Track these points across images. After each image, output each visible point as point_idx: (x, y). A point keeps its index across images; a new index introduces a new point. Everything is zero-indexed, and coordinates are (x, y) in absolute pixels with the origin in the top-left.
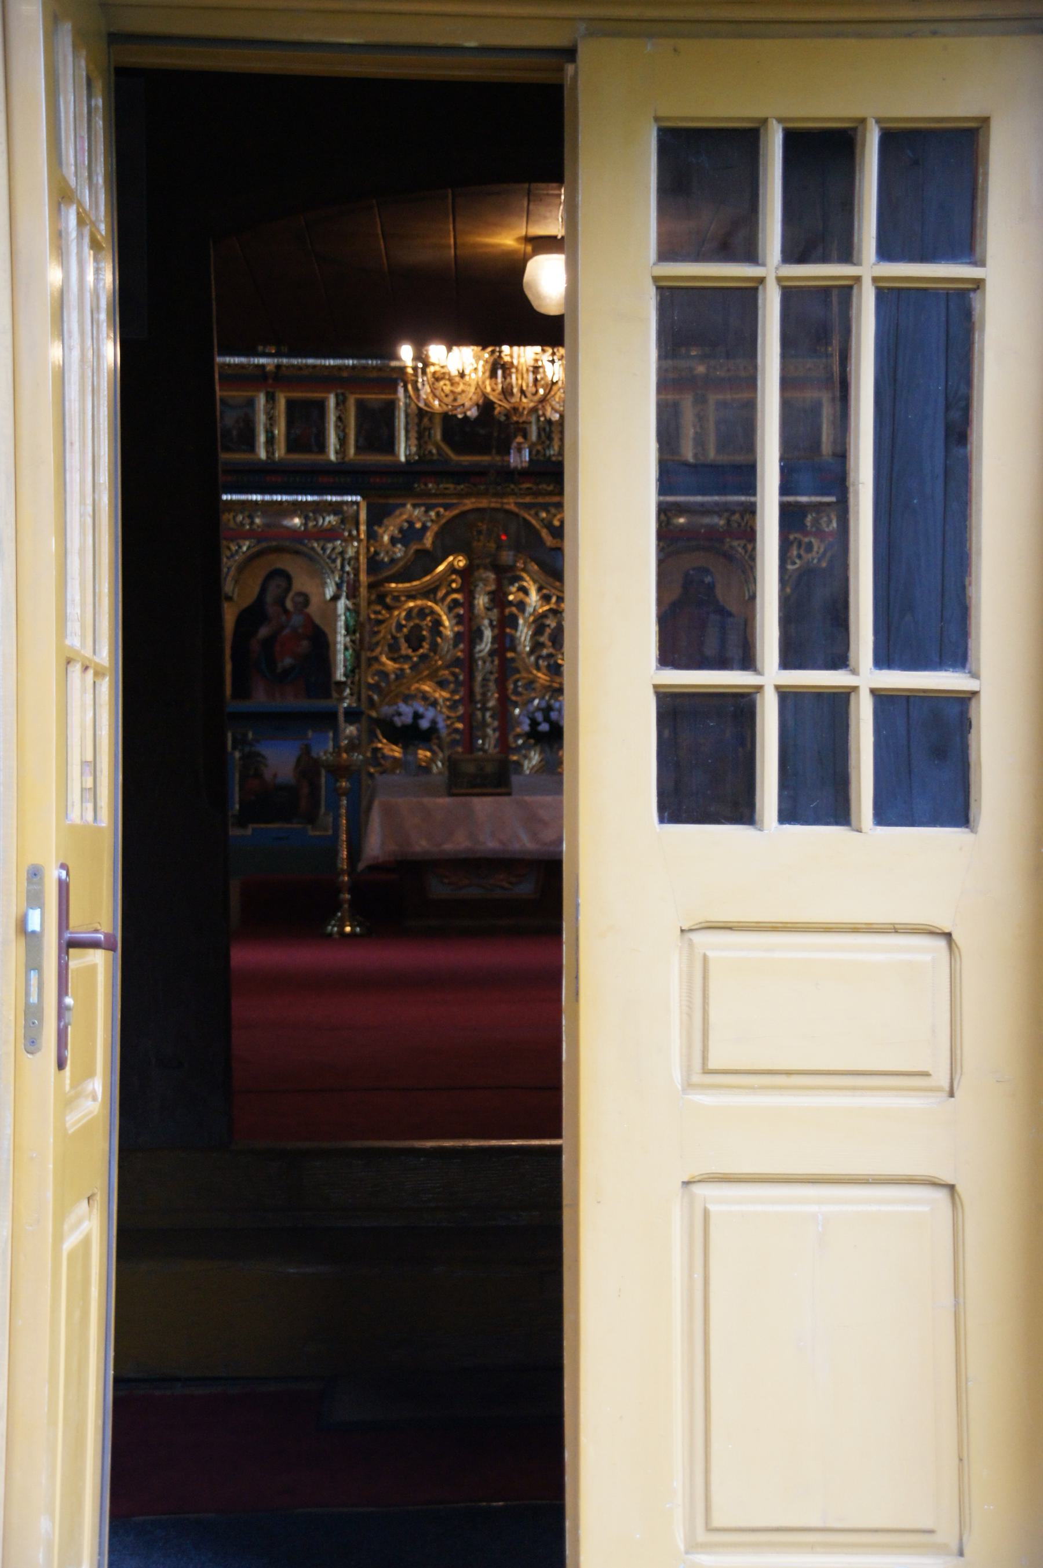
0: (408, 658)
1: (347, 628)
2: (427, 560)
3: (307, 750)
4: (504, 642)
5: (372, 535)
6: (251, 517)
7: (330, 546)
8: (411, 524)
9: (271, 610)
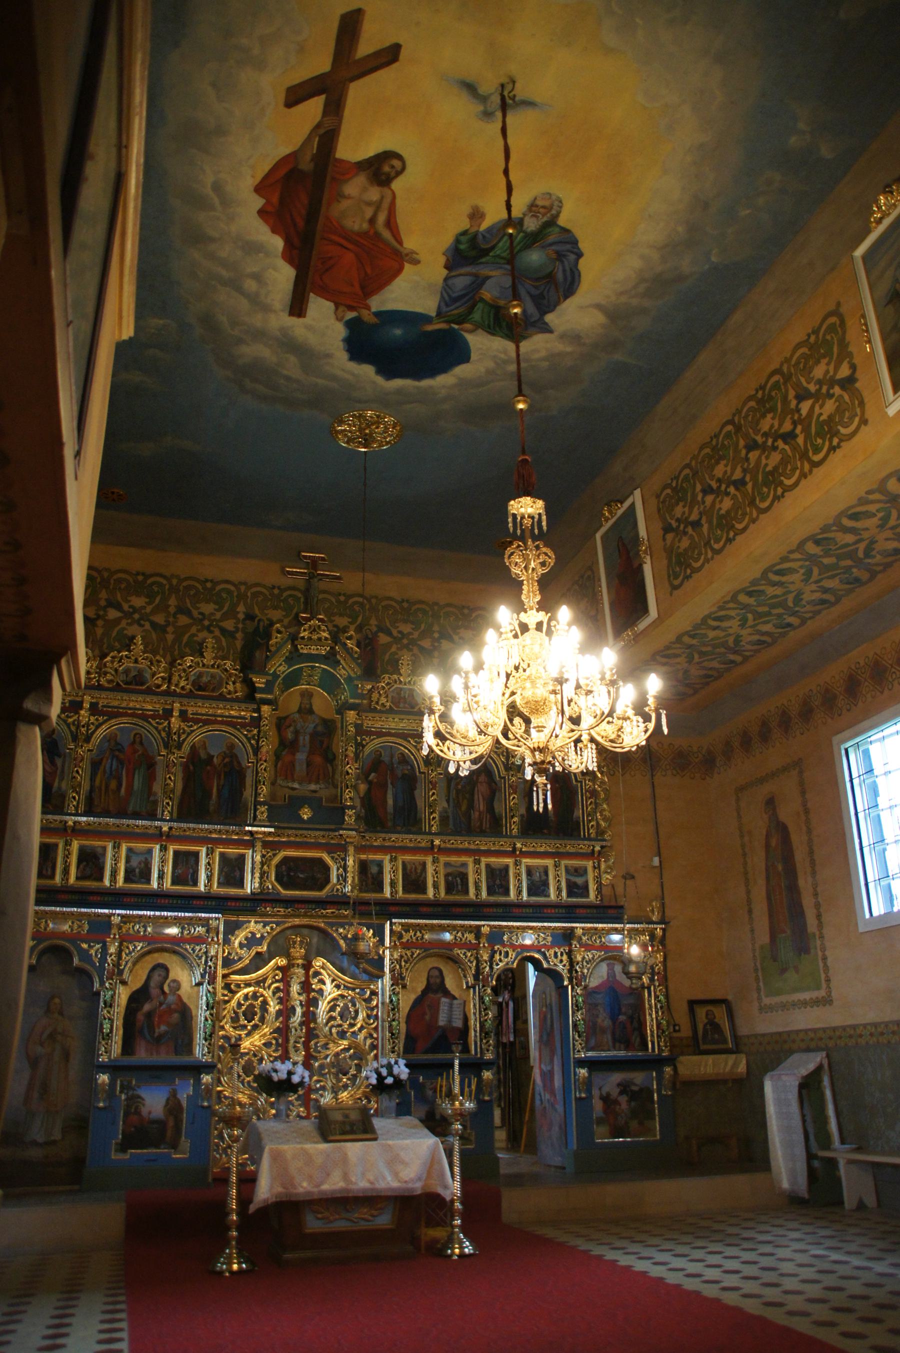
0: (245, 1027)
1: (207, 1006)
2: (259, 961)
3: (174, 1094)
4: (309, 1017)
6: (145, 927)
7: (198, 948)
8: (253, 934)
9: (154, 992)
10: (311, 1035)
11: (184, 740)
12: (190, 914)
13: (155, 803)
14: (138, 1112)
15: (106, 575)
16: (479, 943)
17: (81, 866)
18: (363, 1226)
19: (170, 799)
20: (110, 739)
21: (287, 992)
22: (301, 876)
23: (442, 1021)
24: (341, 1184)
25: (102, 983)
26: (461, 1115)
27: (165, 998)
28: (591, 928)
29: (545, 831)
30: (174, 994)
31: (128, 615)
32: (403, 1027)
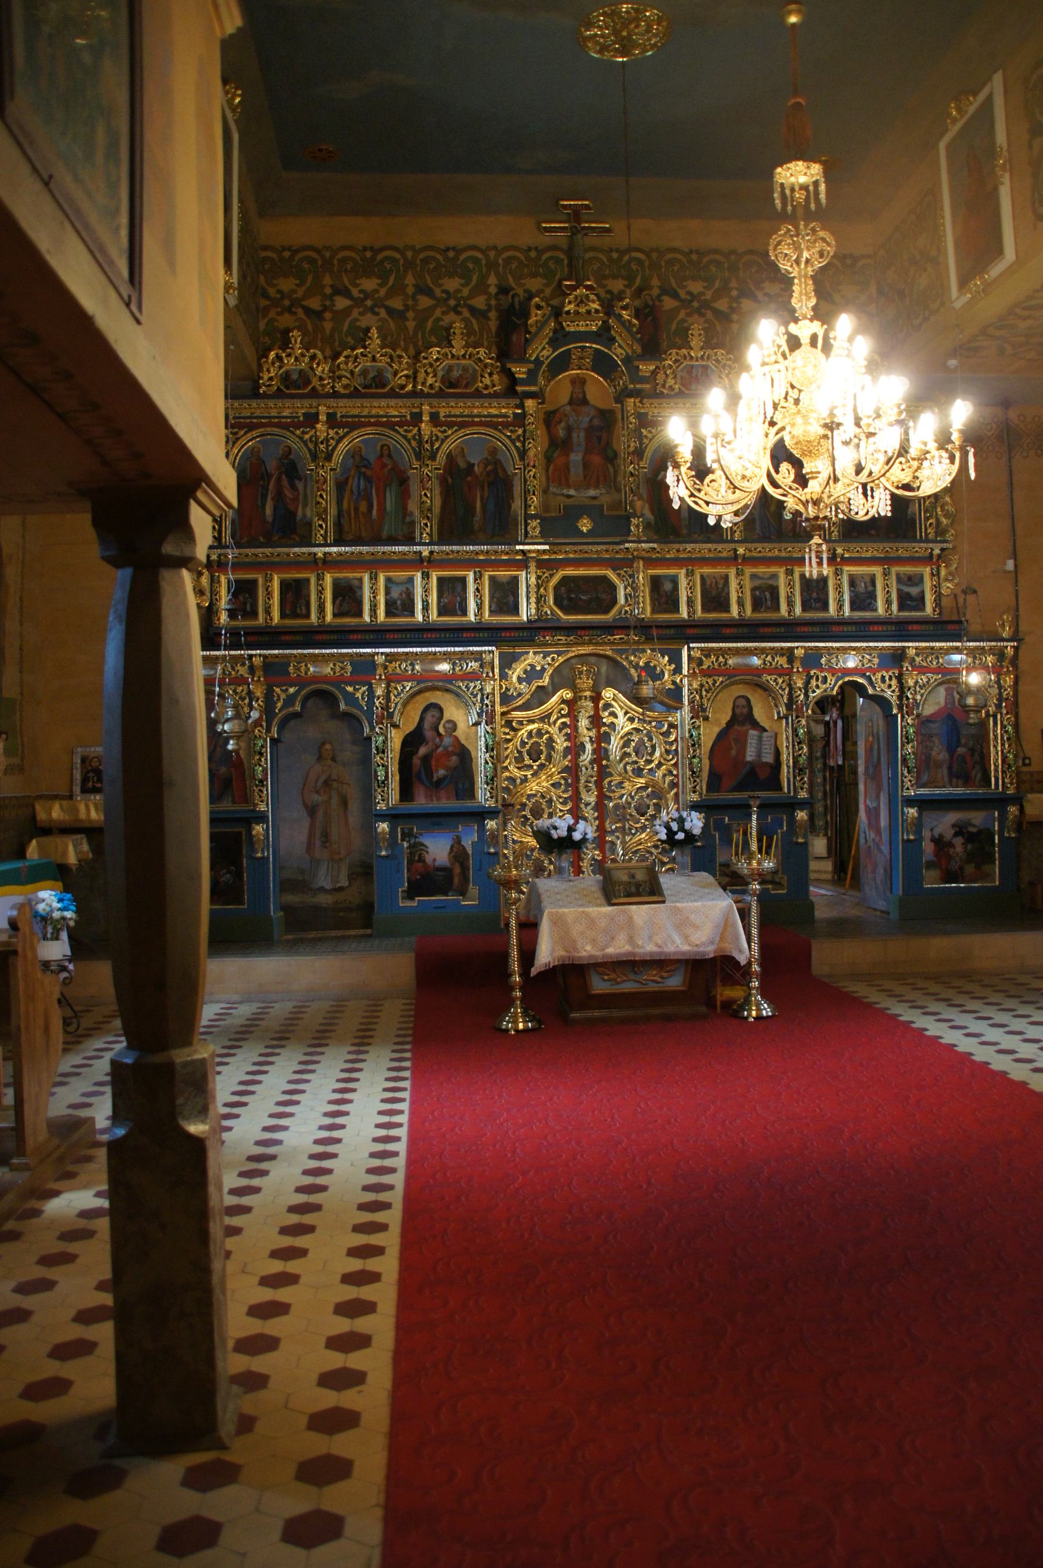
0: (530, 767)
1: (487, 747)
2: (542, 695)
3: (458, 841)
4: (601, 754)
5: (503, 676)
6: (412, 664)
7: (472, 685)
8: (532, 666)
9: (429, 734)
10: (603, 773)
11: (438, 449)
12: (461, 649)
13: (412, 523)
14: (421, 860)
15: (327, 254)
16: (793, 668)
17: (338, 602)
18: (653, 987)
19: (428, 518)
20: (354, 454)
21: (575, 727)
22: (583, 598)
23: (750, 756)
24: (628, 948)
25: (372, 728)
26: (760, 875)
27: (441, 740)
28: (926, 648)
29: (873, 532)
30: (451, 735)
31: (358, 302)
32: (706, 763)
